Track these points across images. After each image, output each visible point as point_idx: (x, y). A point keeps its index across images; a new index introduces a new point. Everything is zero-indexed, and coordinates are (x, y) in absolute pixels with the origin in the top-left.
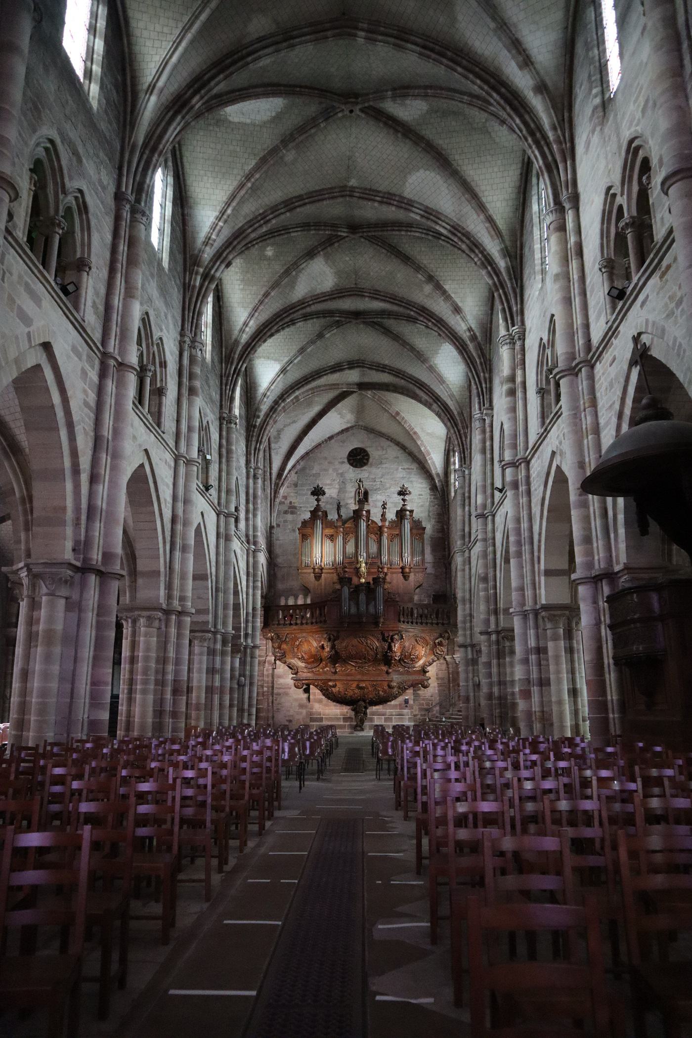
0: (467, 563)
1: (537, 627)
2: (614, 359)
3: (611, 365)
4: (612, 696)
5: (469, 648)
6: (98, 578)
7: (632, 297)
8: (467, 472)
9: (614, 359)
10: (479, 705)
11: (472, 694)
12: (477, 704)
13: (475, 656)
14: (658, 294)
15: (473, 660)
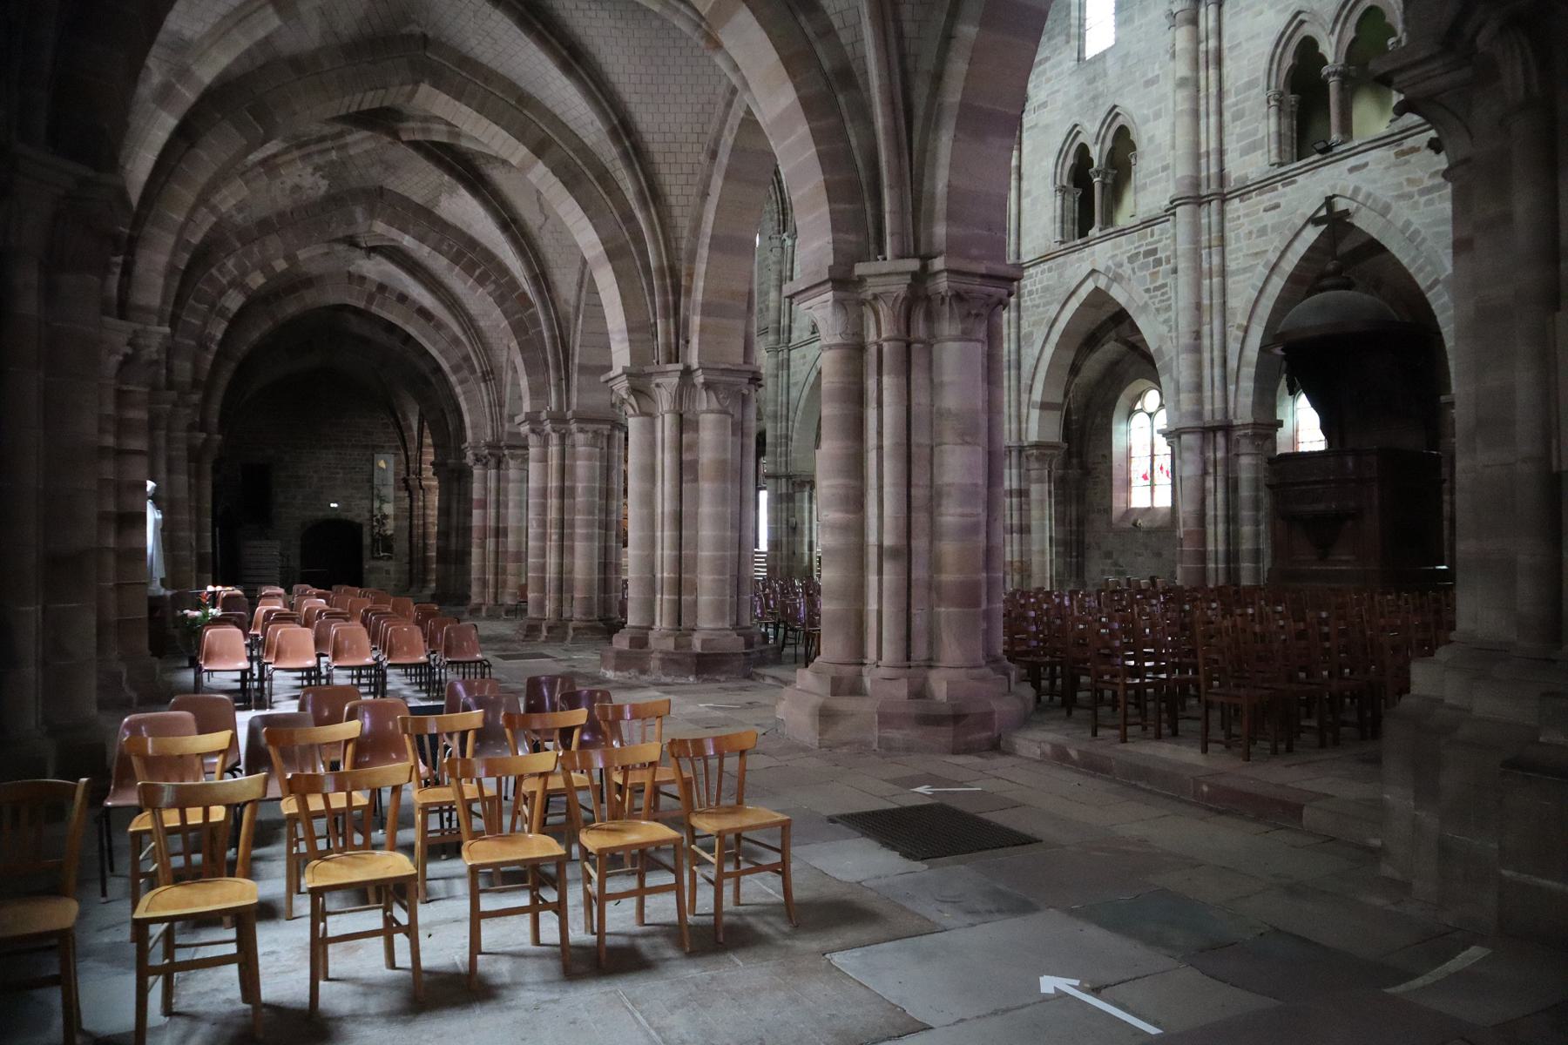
0: (785, 367)
1: (1020, 466)
2: (1277, 206)
3: (1265, 210)
4: (1216, 546)
5: (784, 480)
6: (712, 394)
7: (1338, 157)
8: (789, 242)
9: (1277, 206)
10: (794, 553)
11: (784, 539)
12: (790, 552)
13: (790, 491)
14: (1387, 168)
15: (787, 494)
